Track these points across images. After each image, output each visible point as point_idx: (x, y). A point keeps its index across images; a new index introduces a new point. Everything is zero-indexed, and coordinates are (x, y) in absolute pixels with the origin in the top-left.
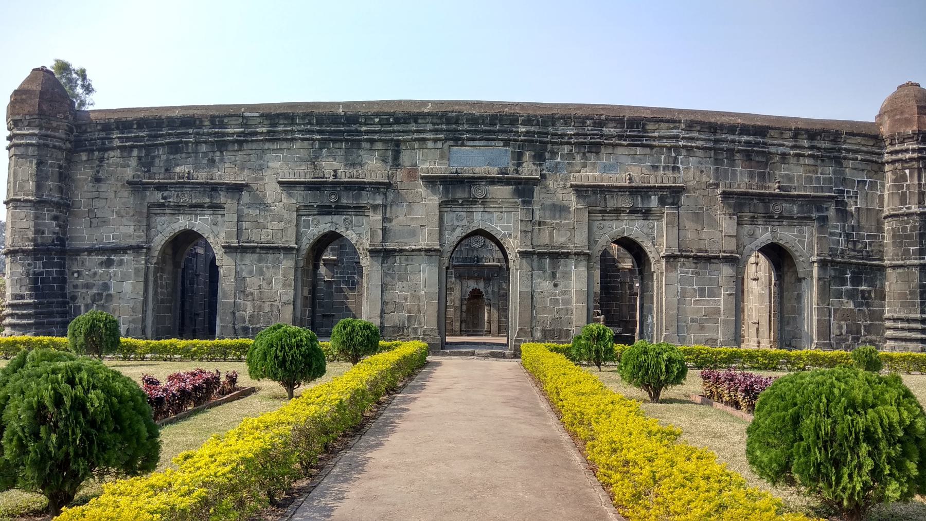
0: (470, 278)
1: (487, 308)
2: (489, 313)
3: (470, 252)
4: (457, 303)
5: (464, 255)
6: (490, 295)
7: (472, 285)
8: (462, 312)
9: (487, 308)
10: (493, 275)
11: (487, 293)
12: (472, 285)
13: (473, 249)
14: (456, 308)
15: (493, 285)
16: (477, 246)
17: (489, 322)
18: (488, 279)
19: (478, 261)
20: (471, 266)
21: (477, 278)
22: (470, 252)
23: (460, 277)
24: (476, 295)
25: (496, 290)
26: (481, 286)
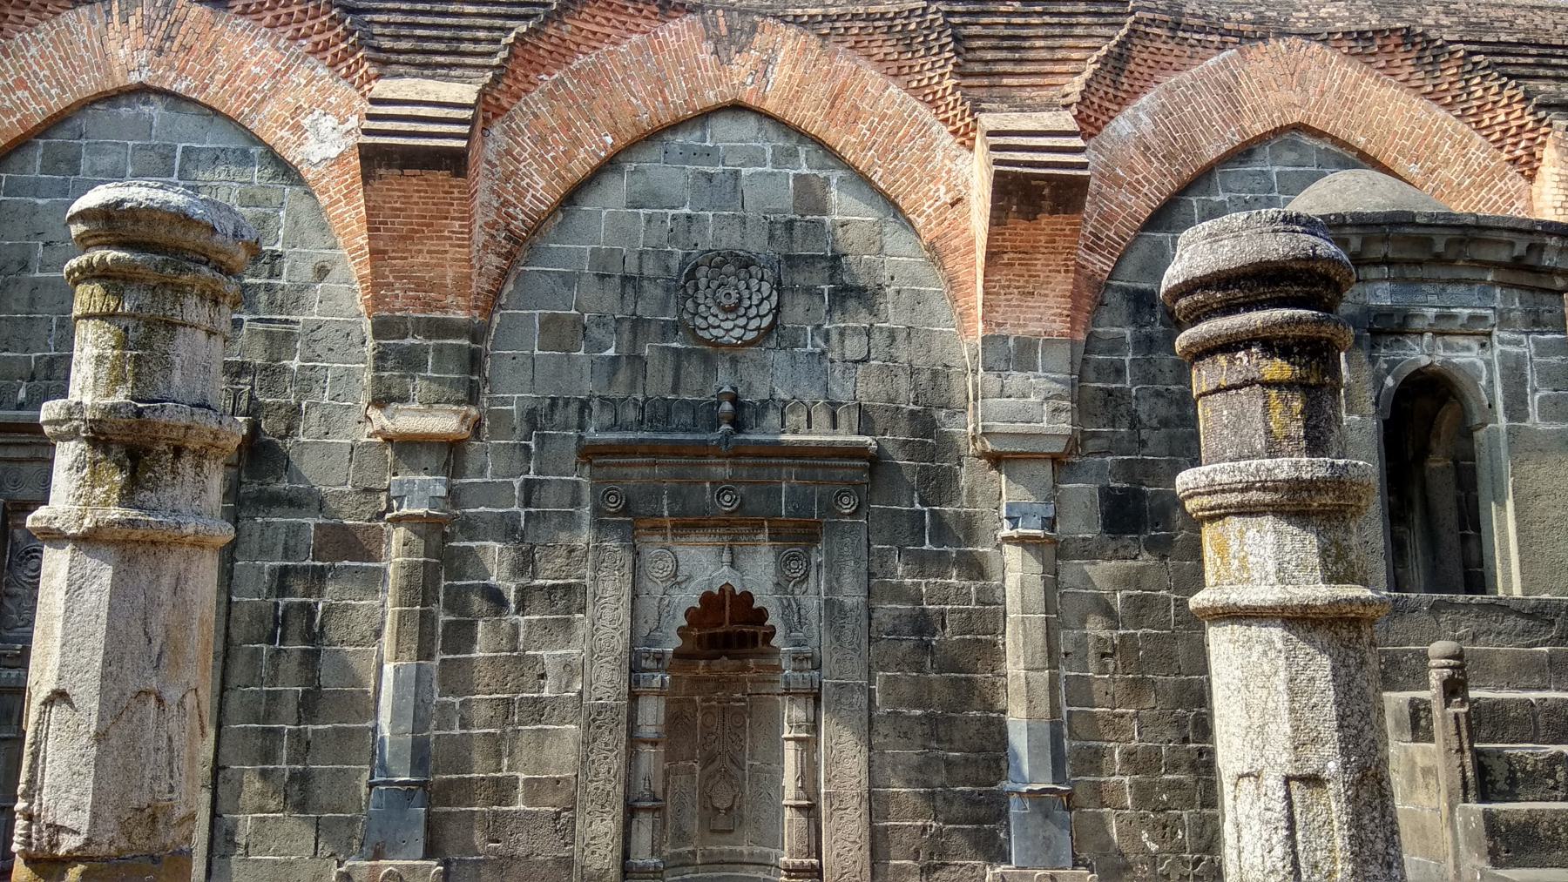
0: (689, 523)
1: (793, 714)
2: (808, 745)
3: (693, 373)
4: (607, 683)
5: (658, 384)
6: (816, 633)
7: (702, 567)
8: (634, 741)
9: (793, 714)
10: (830, 509)
11: (795, 616)
12: (702, 567)
13: (710, 353)
14: (593, 720)
15: (834, 568)
16: (729, 330)
17: (810, 810)
18: (799, 535)
19: (738, 424)
20: (701, 451)
21: (734, 528)
22: (693, 373)
23: (628, 518)
24: (729, 629)
25: (852, 596)
26: (758, 574)
